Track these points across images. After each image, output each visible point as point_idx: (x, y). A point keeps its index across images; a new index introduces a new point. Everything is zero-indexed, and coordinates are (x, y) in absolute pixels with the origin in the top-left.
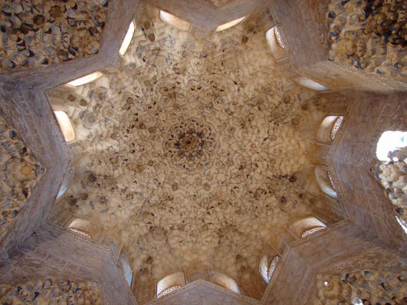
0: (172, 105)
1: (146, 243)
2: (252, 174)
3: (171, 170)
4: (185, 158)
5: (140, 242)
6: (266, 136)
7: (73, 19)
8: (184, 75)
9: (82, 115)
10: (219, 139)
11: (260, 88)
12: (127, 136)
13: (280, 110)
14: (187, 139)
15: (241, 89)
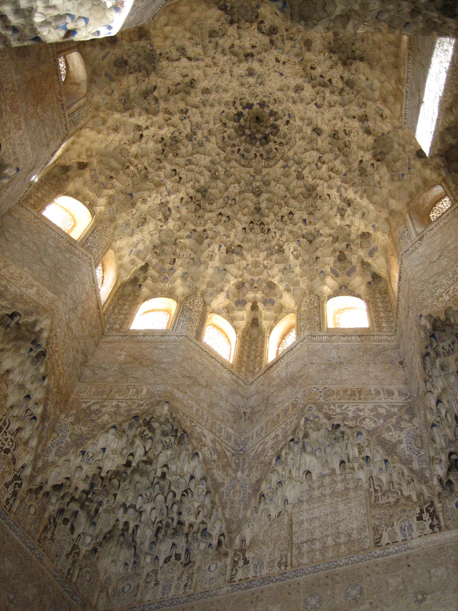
0: (215, 184)
1: (400, 161)
2: (247, 45)
3: (299, 143)
4: (278, 123)
5: (401, 173)
6: (184, 61)
7: (144, 447)
8: (168, 202)
9: (268, 302)
10: (227, 97)
11: (127, 114)
12: (275, 232)
13: (140, 59)
14: (253, 125)
15: (144, 126)
